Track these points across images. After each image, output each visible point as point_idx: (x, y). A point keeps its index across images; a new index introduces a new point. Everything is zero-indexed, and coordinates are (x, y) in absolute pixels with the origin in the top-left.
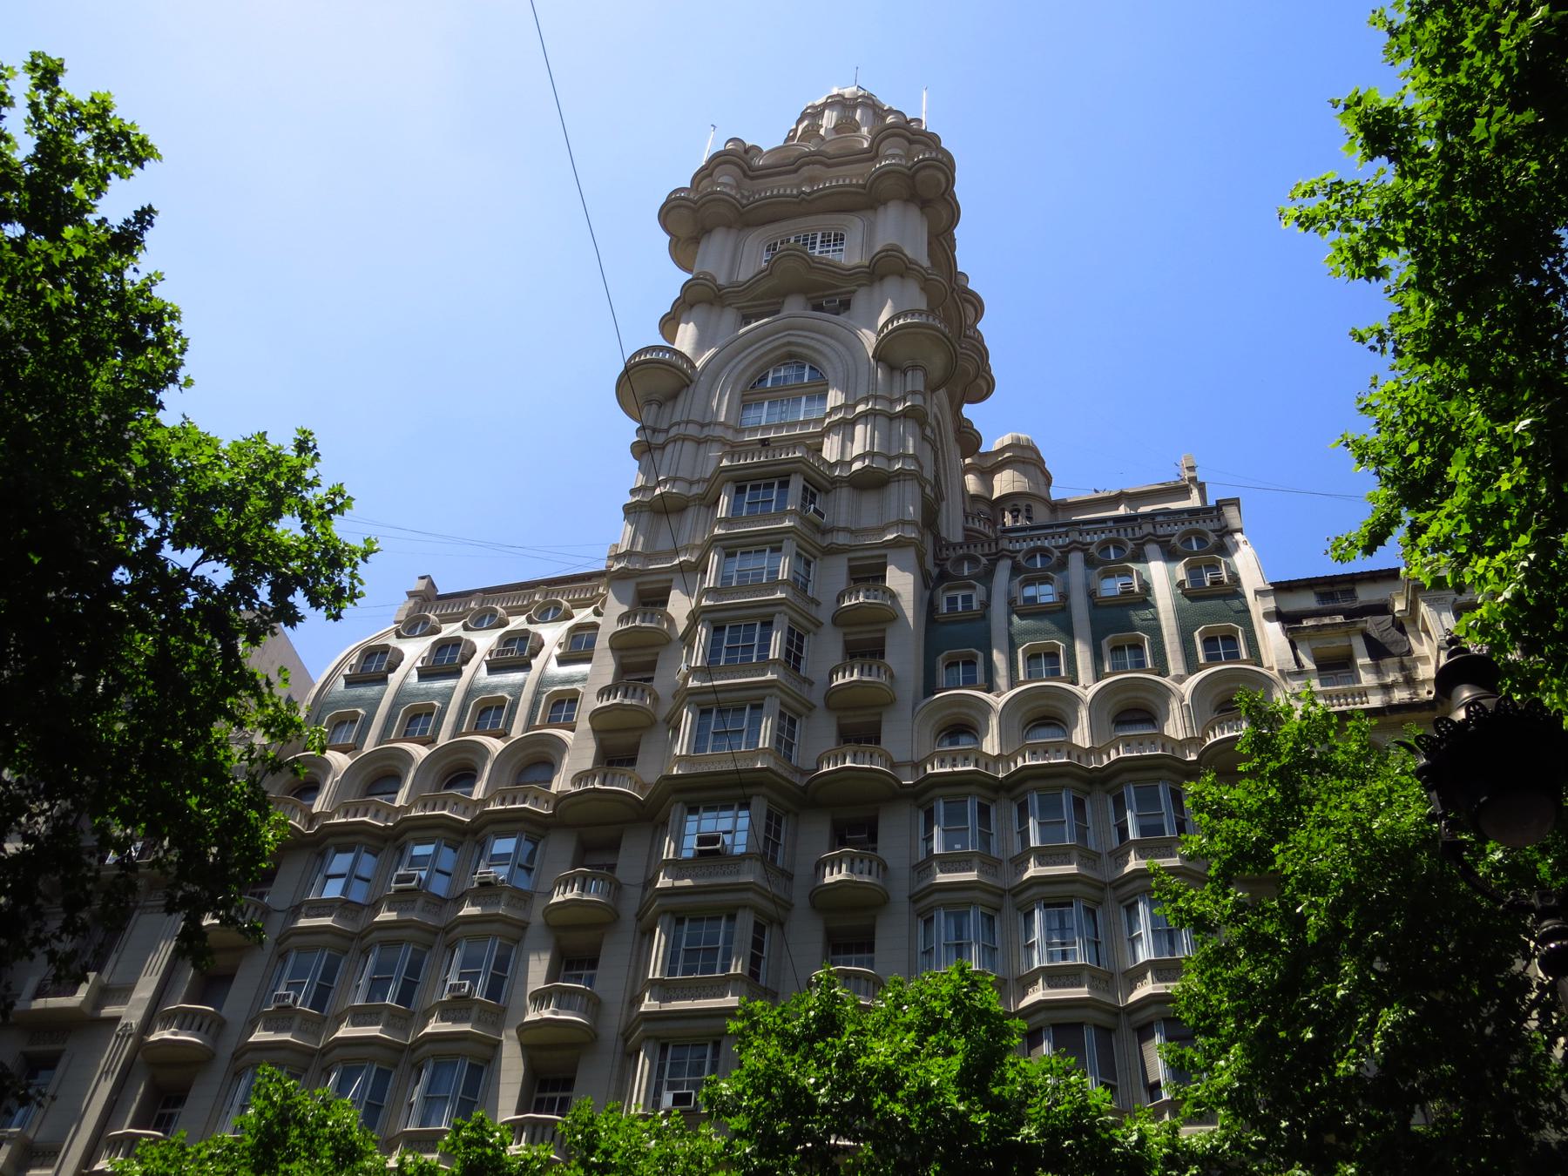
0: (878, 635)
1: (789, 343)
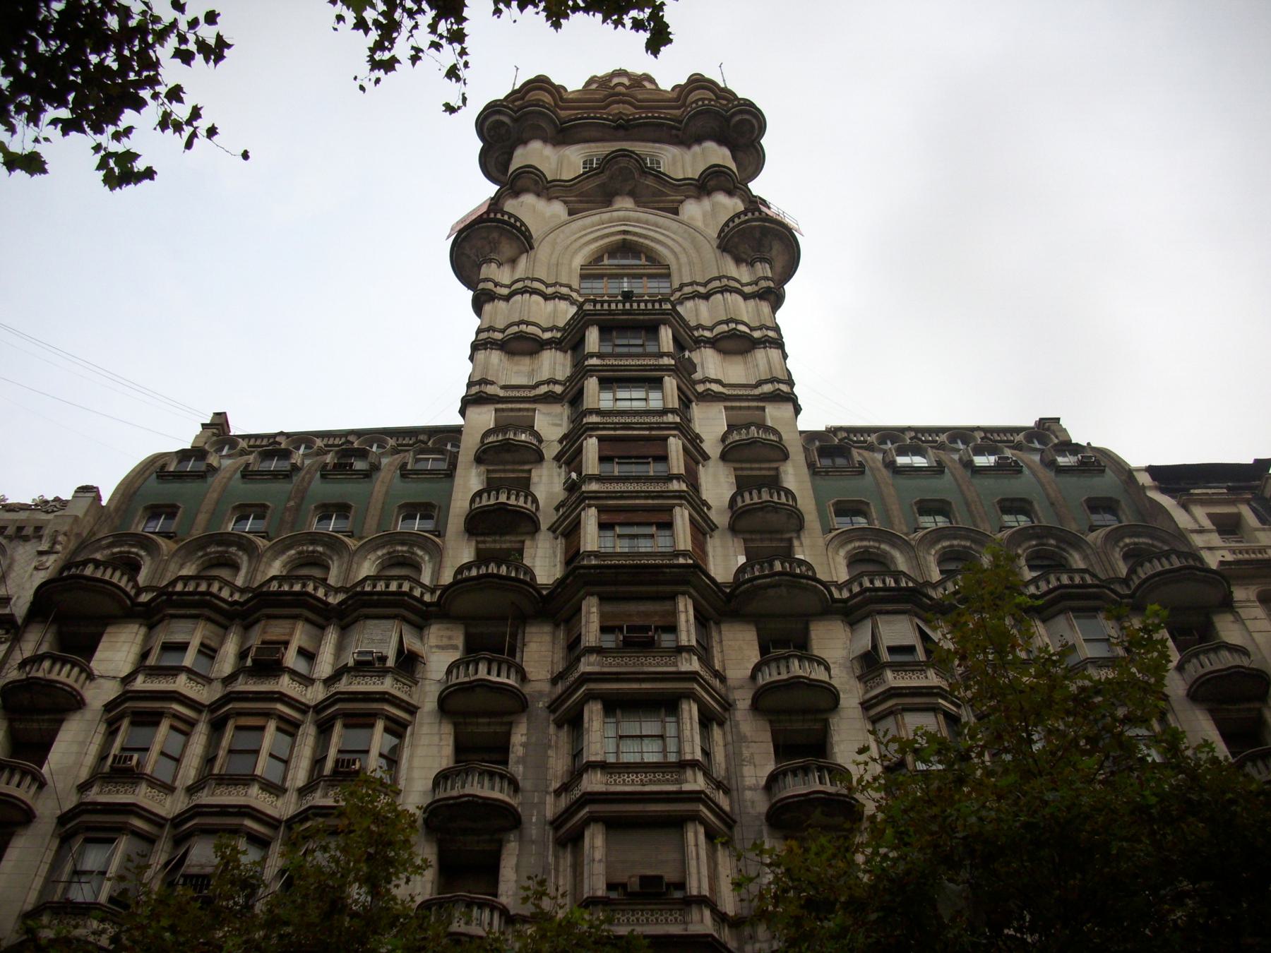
0: (772, 473)
1: (625, 232)
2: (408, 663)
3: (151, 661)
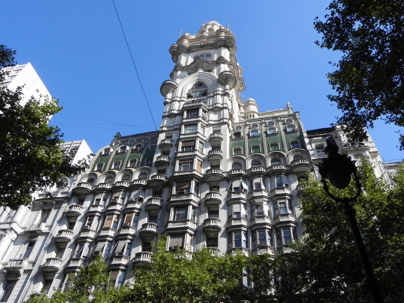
2: (141, 200)
3: (94, 204)
